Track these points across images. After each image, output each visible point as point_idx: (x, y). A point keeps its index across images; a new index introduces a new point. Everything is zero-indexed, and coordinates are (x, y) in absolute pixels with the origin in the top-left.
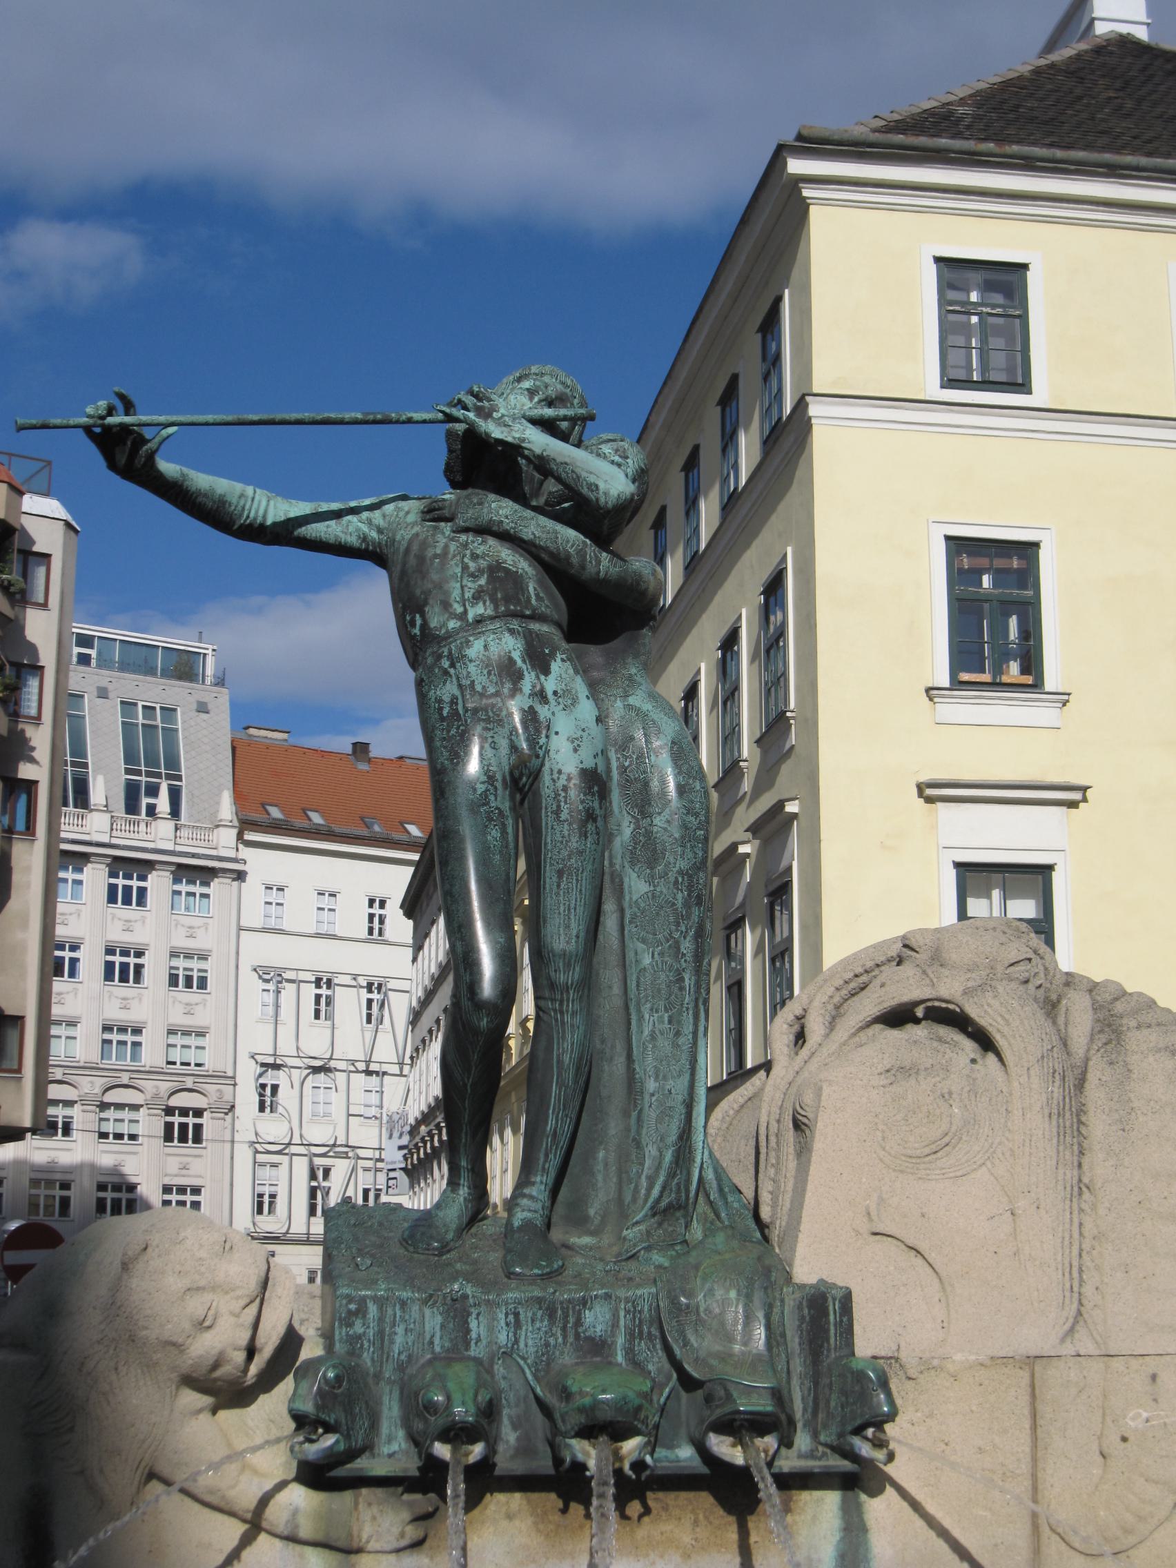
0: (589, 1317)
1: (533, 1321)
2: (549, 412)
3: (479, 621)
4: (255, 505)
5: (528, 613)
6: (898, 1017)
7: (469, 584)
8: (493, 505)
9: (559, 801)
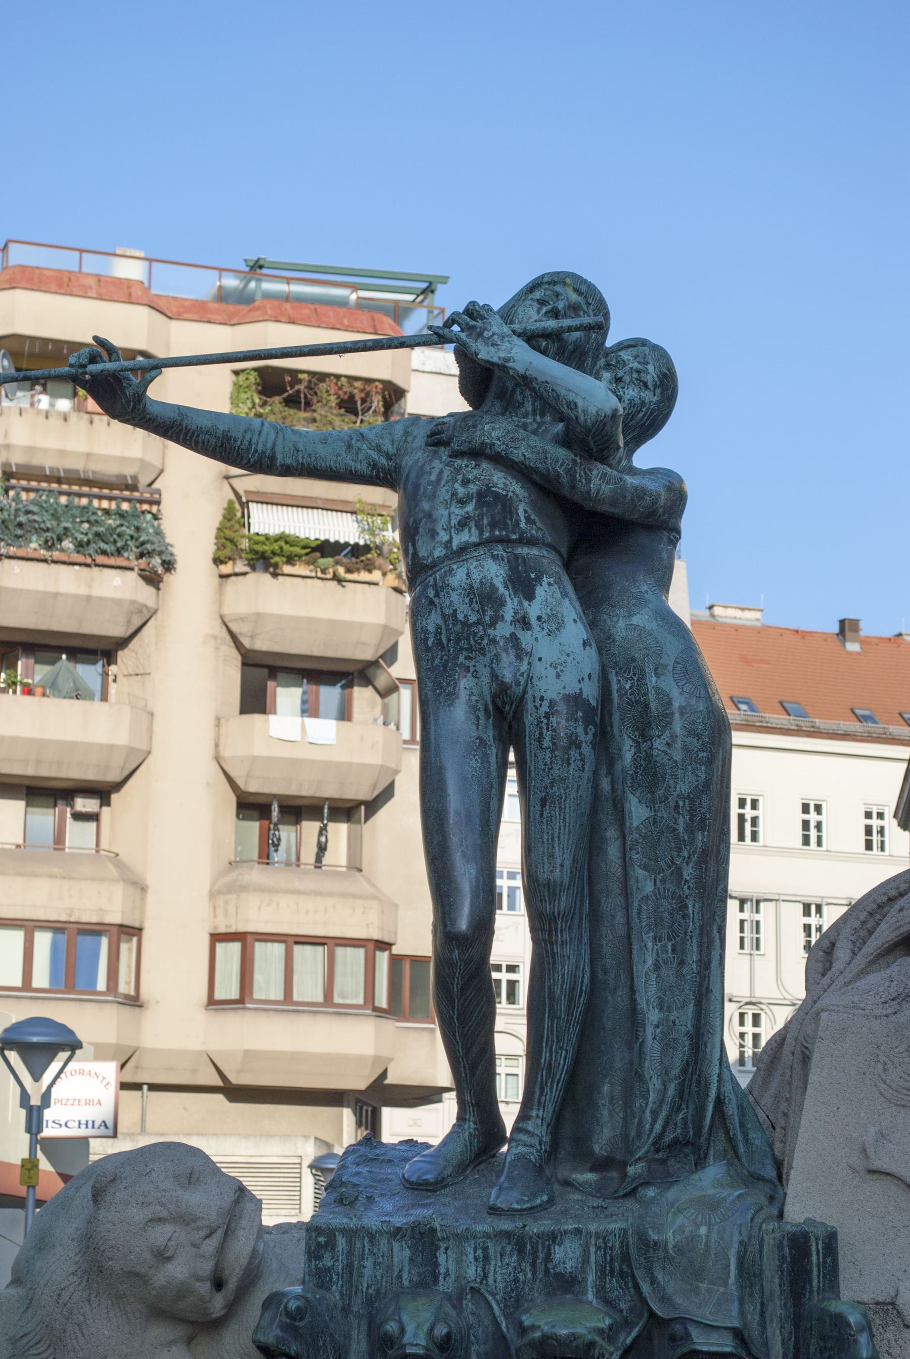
0: (558, 1252)
1: (502, 1255)
2: (552, 324)
3: (464, 549)
4: (263, 438)
5: (514, 537)
7: (457, 511)
8: (487, 427)
9: (541, 728)
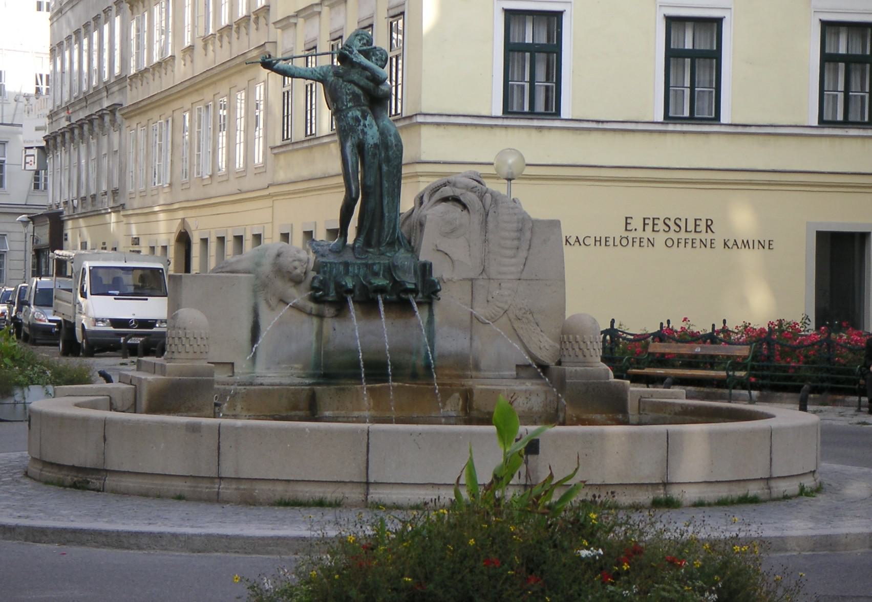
2: (365, 48)
6: (445, 199)
